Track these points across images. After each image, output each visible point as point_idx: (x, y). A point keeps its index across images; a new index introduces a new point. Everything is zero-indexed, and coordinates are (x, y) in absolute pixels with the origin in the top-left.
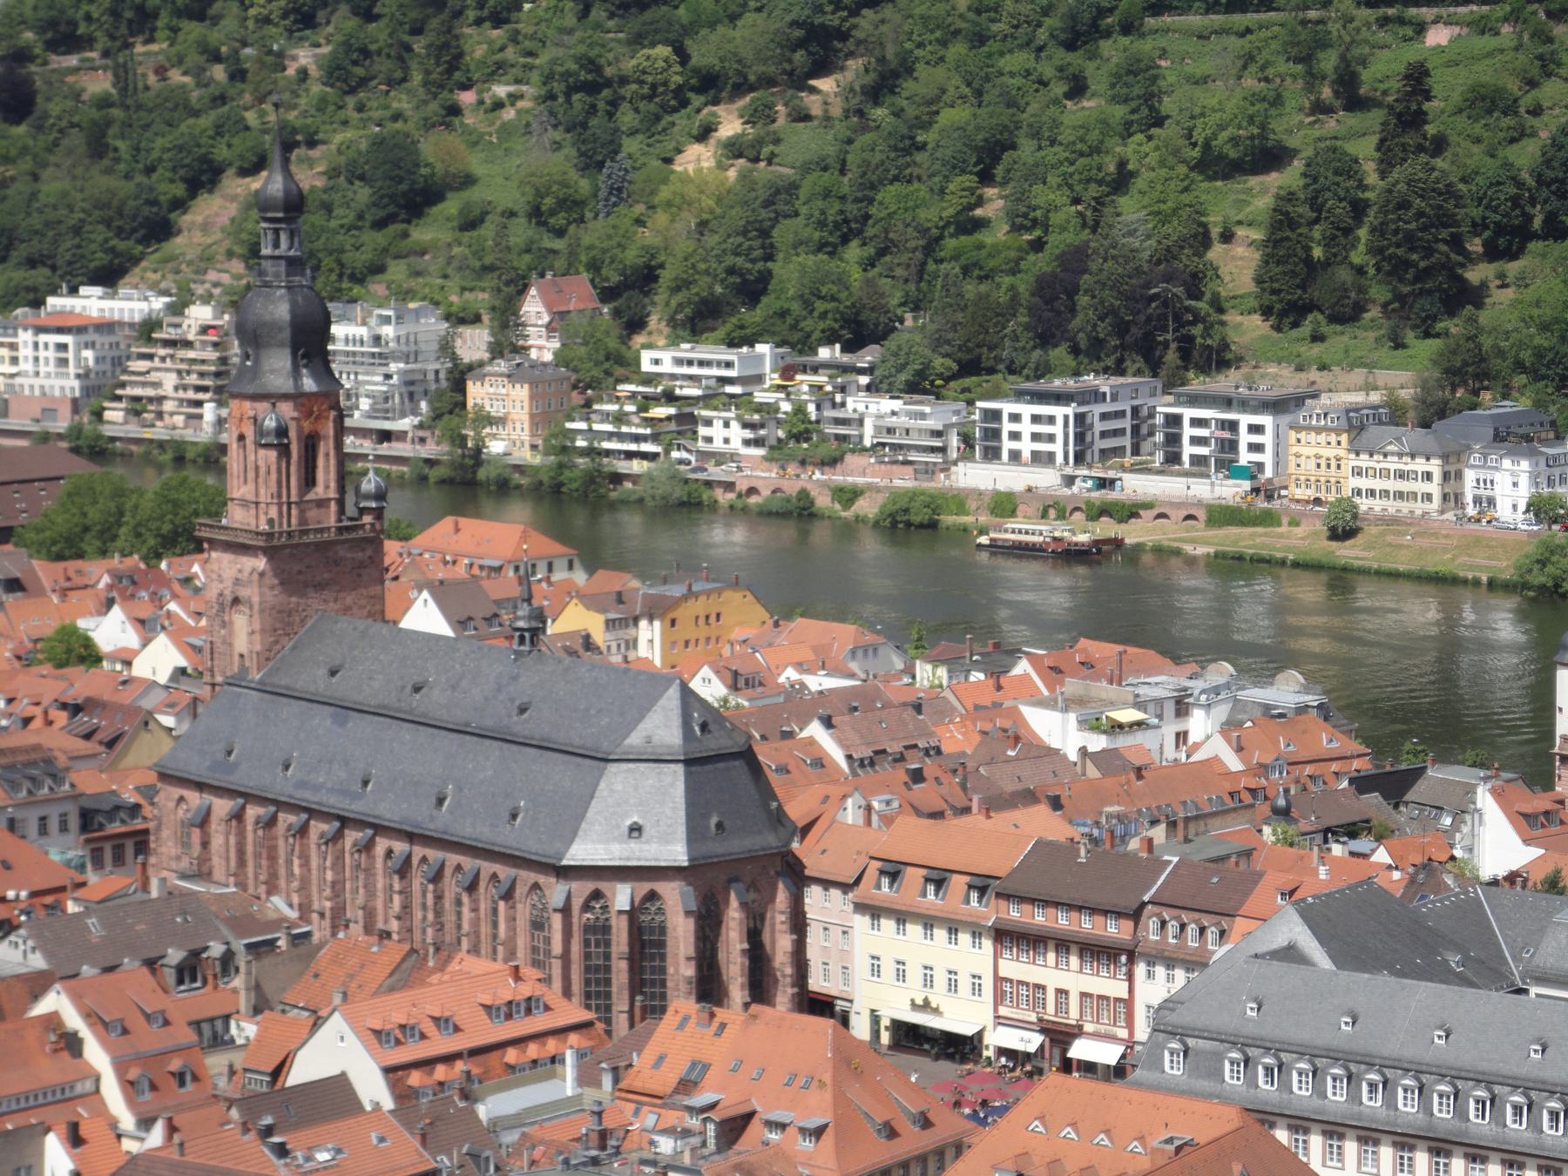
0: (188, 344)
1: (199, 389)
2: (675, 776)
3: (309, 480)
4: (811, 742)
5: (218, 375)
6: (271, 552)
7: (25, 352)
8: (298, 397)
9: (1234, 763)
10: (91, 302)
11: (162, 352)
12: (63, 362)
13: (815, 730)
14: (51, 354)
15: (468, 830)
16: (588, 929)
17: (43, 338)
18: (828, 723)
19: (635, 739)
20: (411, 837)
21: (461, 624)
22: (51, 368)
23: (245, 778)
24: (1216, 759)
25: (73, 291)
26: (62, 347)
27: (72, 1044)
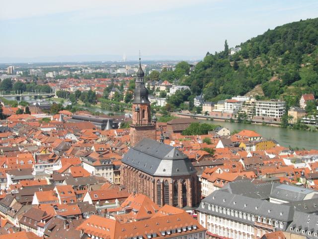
0: (250, 105)
1: (251, 112)
2: (171, 162)
3: (143, 117)
4: (240, 162)
5: (253, 110)
6: (136, 128)
7: (226, 106)
8: (142, 104)
9: (310, 169)
10: (238, 98)
11: (246, 106)
12: (231, 108)
13: (241, 161)
14: (230, 106)
15: (147, 170)
16: (158, 185)
17: (228, 104)
18: (243, 159)
19: (167, 156)
20: (141, 171)
21: (225, 145)
22: (229, 108)
23: (128, 162)
24: (308, 168)
25: (236, 97)
26: (231, 105)
27: (56, 195)
